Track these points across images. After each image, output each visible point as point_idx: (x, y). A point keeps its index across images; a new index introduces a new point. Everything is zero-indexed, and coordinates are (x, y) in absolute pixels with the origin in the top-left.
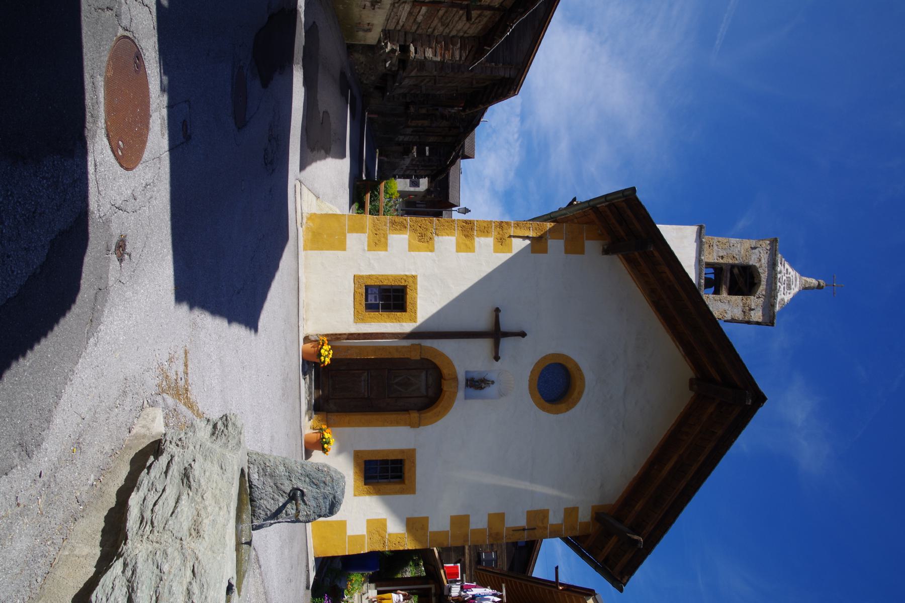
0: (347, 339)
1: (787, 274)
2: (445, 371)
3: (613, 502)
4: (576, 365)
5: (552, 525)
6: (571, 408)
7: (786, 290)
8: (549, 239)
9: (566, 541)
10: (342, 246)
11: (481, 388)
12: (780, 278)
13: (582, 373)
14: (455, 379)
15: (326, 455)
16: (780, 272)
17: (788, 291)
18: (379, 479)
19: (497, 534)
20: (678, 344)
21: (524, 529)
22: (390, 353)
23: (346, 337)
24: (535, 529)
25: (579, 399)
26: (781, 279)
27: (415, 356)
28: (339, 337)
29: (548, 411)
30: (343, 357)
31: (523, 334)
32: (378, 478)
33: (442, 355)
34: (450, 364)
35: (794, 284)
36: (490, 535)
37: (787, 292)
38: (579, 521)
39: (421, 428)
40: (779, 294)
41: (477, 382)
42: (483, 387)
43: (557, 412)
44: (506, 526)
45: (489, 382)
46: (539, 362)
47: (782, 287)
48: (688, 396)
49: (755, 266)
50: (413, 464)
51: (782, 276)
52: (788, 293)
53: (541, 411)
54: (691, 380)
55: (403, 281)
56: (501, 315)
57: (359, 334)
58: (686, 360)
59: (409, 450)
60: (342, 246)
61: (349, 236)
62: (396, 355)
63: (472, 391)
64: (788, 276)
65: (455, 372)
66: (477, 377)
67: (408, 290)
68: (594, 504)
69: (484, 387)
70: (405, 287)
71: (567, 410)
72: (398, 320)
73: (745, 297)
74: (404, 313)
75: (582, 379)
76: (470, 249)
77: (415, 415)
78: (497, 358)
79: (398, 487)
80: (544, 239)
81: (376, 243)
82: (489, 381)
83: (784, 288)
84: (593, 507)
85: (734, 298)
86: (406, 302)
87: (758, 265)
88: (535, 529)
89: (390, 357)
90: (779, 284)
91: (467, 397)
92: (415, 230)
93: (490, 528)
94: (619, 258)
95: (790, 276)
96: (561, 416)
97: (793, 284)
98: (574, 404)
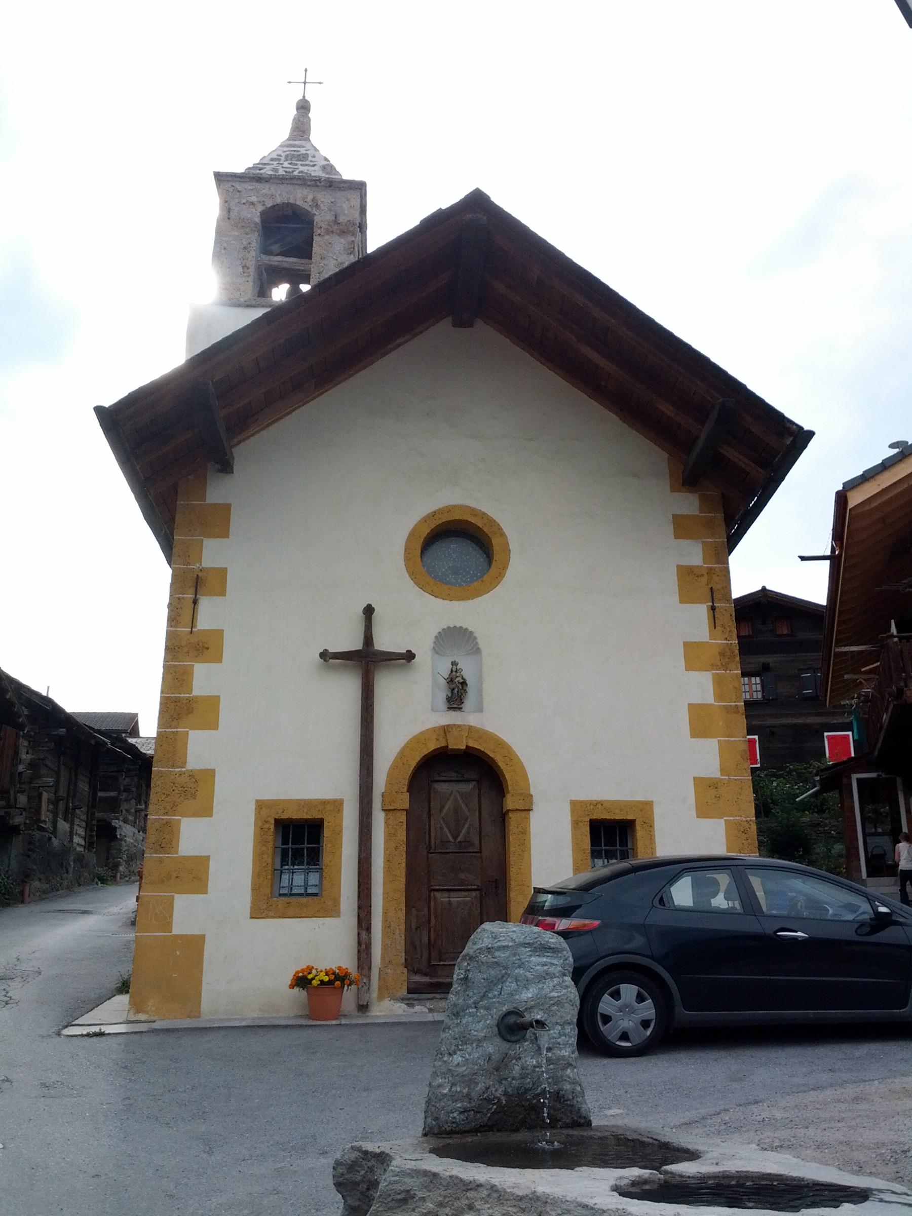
0: (369, 929)
1: (280, 160)
2: (432, 746)
3: (667, 455)
4: (425, 520)
5: (704, 559)
6: (500, 529)
7: (307, 163)
8: (201, 565)
9: (733, 541)
10: (195, 944)
11: (464, 683)
12: (286, 172)
13: (440, 509)
14: (445, 730)
15: (589, 861)
16: (276, 170)
17: (310, 158)
18: (627, 846)
19: (722, 654)
20: (390, 346)
21: (713, 608)
22: (396, 848)
23: (364, 933)
24: (711, 589)
25: (484, 515)
26: (288, 170)
27: (404, 800)
28: (363, 946)
29: (505, 568)
30: (403, 936)
31: (369, 611)
32: (624, 848)
33: (402, 754)
34: (417, 740)
35: (299, 149)
36: (725, 667)
37: (311, 161)
38: (697, 513)
39: (532, 791)
40: (313, 174)
41: (453, 690)
42: (462, 681)
43: (507, 551)
44: (708, 640)
45: (454, 669)
46: (417, 584)
47: (302, 168)
48: (483, 330)
49: (263, 213)
50: (599, 806)
51: (283, 167)
52: (313, 159)
53: (504, 579)
54: (456, 324)
55: (267, 826)
56: (332, 650)
57: (359, 907)
58: (421, 332)
59: (573, 811)
60: (195, 944)
61: (176, 930)
62: (402, 835)
63: (470, 701)
64: (283, 158)
65: (434, 730)
66: (442, 694)
67: (283, 817)
68: (668, 488)
69: (463, 678)
70: (278, 822)
71: (503, 535)
72: (338, 833)
73: (317, 231)
74: (326, 824)
75: (449, 509)
76: (213, 703)
77: (510, 802)
78: (409, 656)
79: (640, 832)
80: (200, 574)
81: (194, 878)
82: (452, 671)
83: (301, 165)
84: (673, 489)
85: (316, 249)
86: (306, 820)
87: (260, 208)
88: (711, 589)
89: (404, 847)
90: (296, 173)
91: (480, 710)
92: (174, 805)
93: (713, 666)
94: (239, 442)
95: (283, 155)
96: (512, 546)
97: (298, 151)
98: (492, 522)
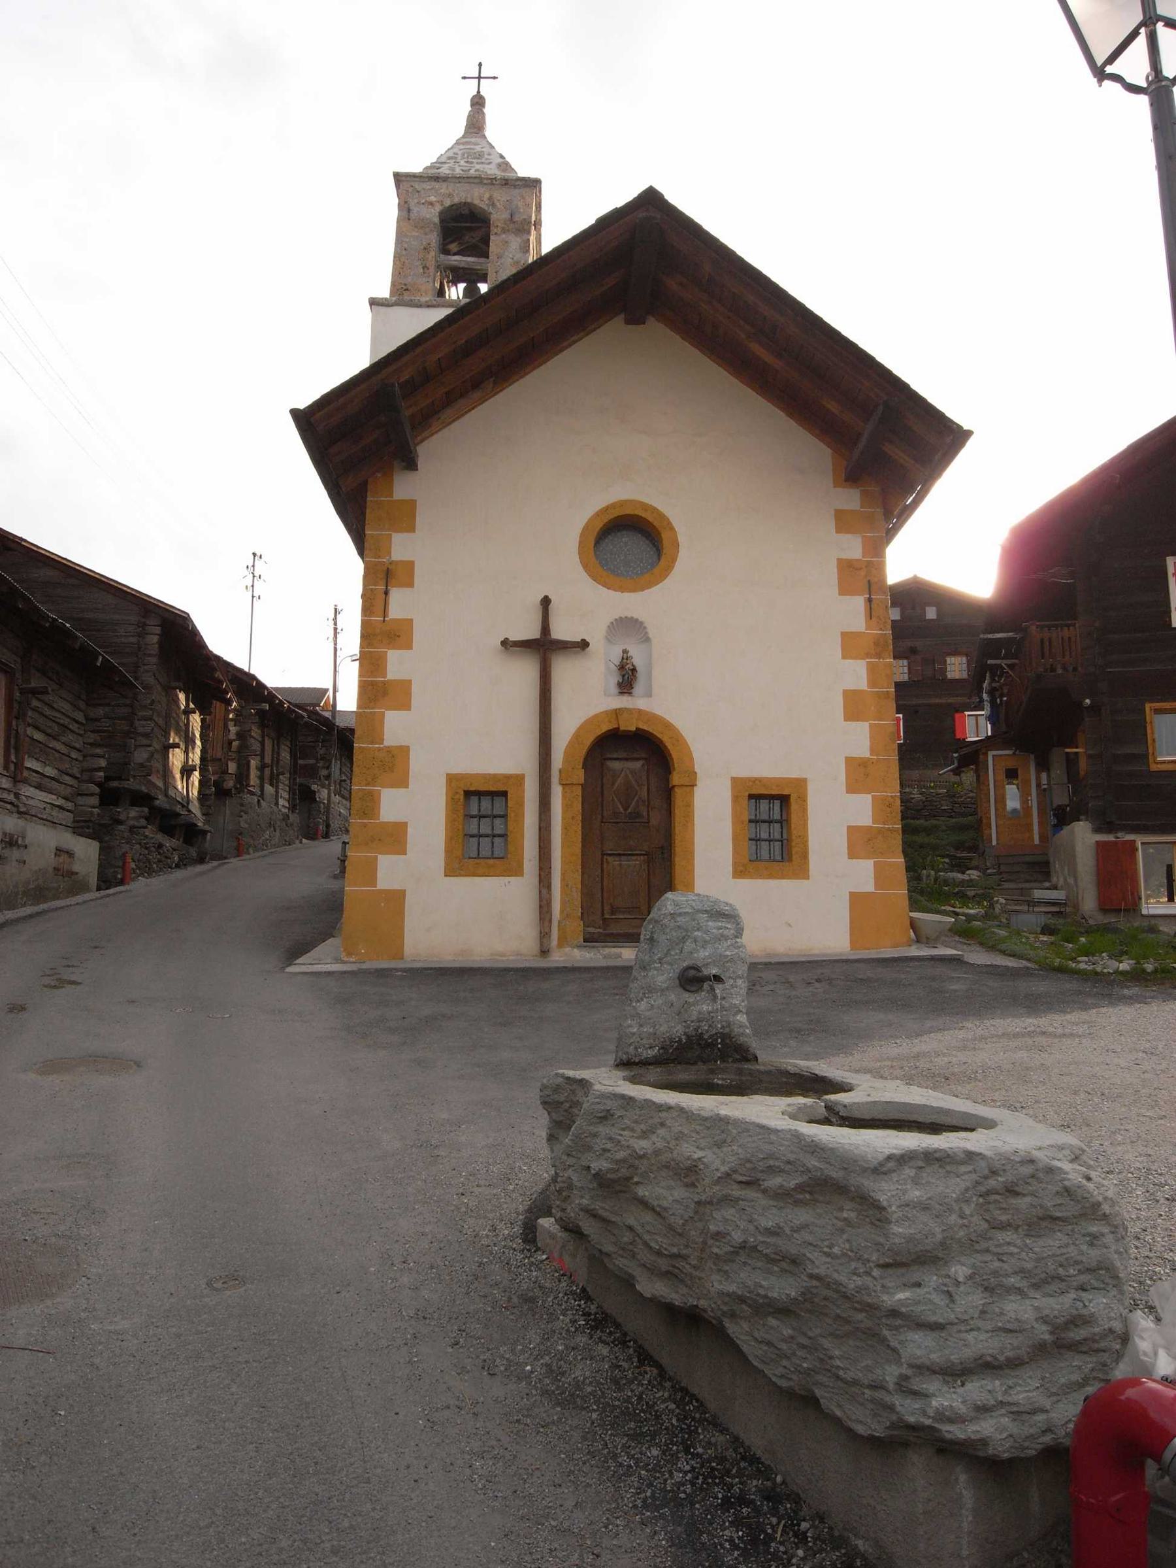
0: (549, 887)
1: (456, 158)
2: (605, 728)
3: (829, 451)
4: (598, 514)
6: (669, 523)
7: (483, 160)
8: (390, 557)
10: (397, 898)
11: (634, 670)
12: (463, 170)
13: (612, 504)
14: (617, 713)
16: (453, 169)
17: (486, 156)
19: (876, 644)
20: (565, 344)
21: (870, 600)
22: (573, 818)
23: (544, 891)
24: (869, 581)
25: (654, 510)
26: (463, 168)
27: (579, 775)
28: (545, 902)
29: (674, 560)
31: (546, 602)
33: (577, 736)
35: (472, 147)
36: (879, 655)
37: (487, 159)
38: (858, 508)
40: (489, 172)
41: (623, 676)
43: (676, 545)
45: (625, 657)
47: (478, 167)
48: (654, 328)
49: (441, 213)
50: (757, 782)
51: (459, 166)
52: (489, 157)
54: (628, 322)
55: (457, 796)
58: (595, 330)
60: (397, 898)
62: (578, 806)
63: (639, 687)
64: (459, 157)
65: (606, 712)
66: (614, 679)
69: (633, 665)
71: (672, 529)
72: (521, 804)
73: (493, 230)
75: (622, 504)
77: (676, 779)
78: (584, 645)
80: (390, 567)
82: (623, 658)
83: (477, 163)
85: (493, 248)
87: (438, 208)
88: (869, 581)
90: (472, 172)
91: (649, 694)
92: (374, 778)
93: (868, 655)
94: (422, 441)
95: (460, 153)
96: (681, 539)
97: (473, 149)
98: (662, 517)
